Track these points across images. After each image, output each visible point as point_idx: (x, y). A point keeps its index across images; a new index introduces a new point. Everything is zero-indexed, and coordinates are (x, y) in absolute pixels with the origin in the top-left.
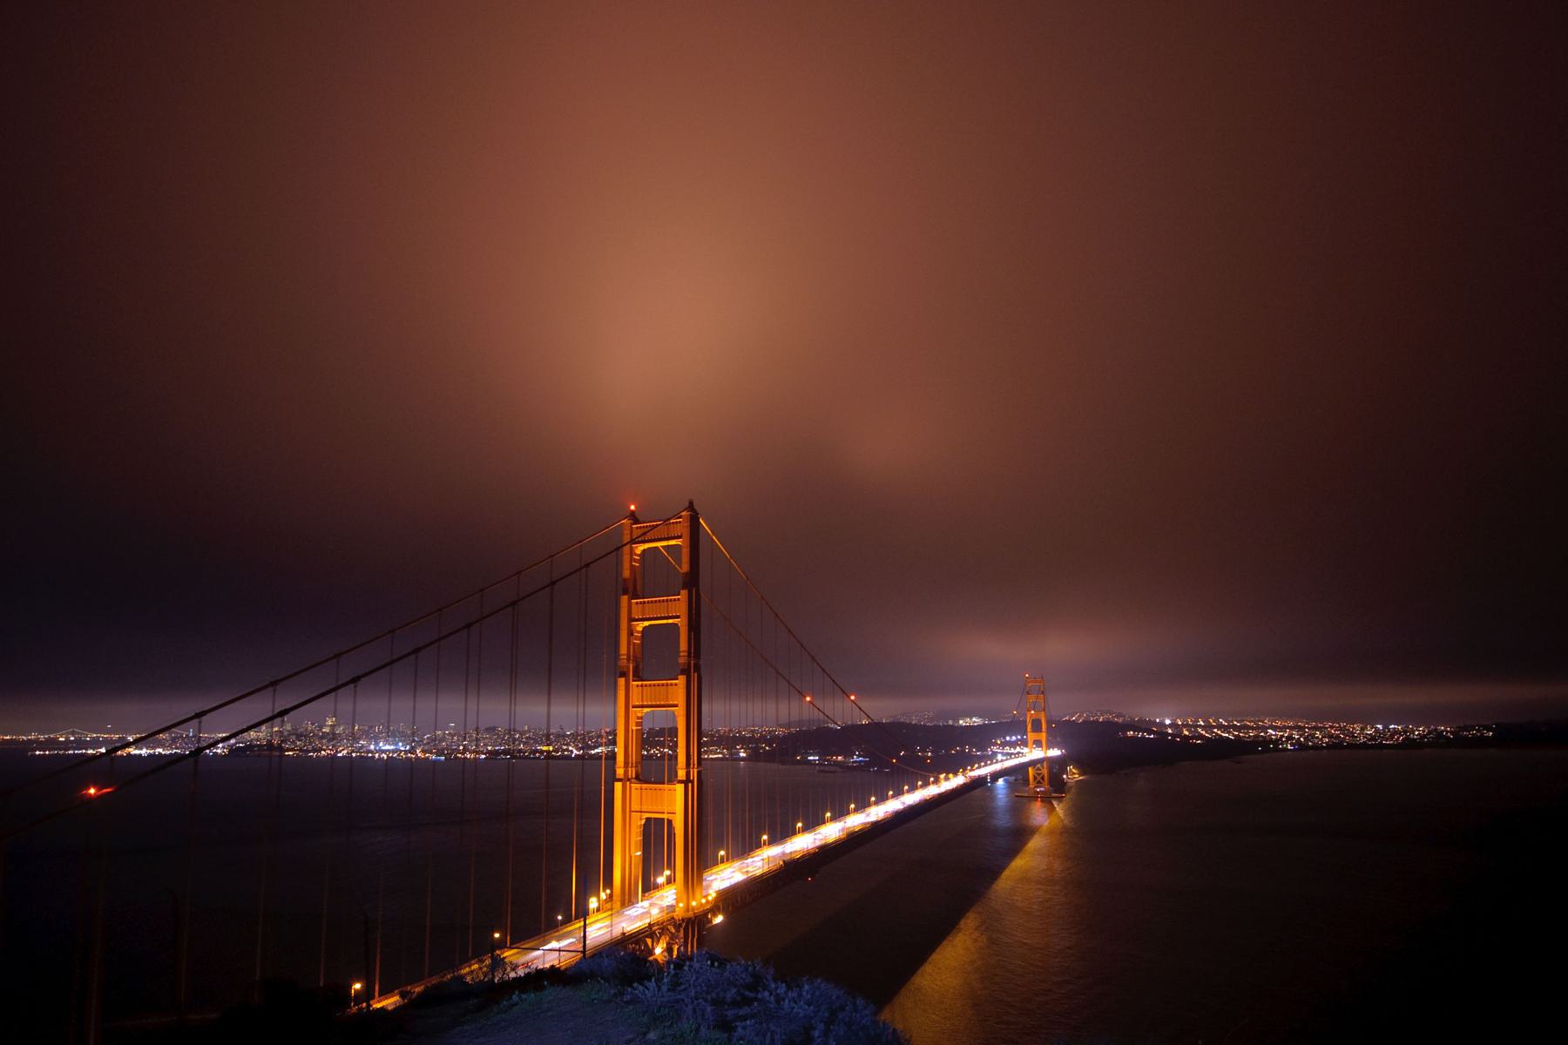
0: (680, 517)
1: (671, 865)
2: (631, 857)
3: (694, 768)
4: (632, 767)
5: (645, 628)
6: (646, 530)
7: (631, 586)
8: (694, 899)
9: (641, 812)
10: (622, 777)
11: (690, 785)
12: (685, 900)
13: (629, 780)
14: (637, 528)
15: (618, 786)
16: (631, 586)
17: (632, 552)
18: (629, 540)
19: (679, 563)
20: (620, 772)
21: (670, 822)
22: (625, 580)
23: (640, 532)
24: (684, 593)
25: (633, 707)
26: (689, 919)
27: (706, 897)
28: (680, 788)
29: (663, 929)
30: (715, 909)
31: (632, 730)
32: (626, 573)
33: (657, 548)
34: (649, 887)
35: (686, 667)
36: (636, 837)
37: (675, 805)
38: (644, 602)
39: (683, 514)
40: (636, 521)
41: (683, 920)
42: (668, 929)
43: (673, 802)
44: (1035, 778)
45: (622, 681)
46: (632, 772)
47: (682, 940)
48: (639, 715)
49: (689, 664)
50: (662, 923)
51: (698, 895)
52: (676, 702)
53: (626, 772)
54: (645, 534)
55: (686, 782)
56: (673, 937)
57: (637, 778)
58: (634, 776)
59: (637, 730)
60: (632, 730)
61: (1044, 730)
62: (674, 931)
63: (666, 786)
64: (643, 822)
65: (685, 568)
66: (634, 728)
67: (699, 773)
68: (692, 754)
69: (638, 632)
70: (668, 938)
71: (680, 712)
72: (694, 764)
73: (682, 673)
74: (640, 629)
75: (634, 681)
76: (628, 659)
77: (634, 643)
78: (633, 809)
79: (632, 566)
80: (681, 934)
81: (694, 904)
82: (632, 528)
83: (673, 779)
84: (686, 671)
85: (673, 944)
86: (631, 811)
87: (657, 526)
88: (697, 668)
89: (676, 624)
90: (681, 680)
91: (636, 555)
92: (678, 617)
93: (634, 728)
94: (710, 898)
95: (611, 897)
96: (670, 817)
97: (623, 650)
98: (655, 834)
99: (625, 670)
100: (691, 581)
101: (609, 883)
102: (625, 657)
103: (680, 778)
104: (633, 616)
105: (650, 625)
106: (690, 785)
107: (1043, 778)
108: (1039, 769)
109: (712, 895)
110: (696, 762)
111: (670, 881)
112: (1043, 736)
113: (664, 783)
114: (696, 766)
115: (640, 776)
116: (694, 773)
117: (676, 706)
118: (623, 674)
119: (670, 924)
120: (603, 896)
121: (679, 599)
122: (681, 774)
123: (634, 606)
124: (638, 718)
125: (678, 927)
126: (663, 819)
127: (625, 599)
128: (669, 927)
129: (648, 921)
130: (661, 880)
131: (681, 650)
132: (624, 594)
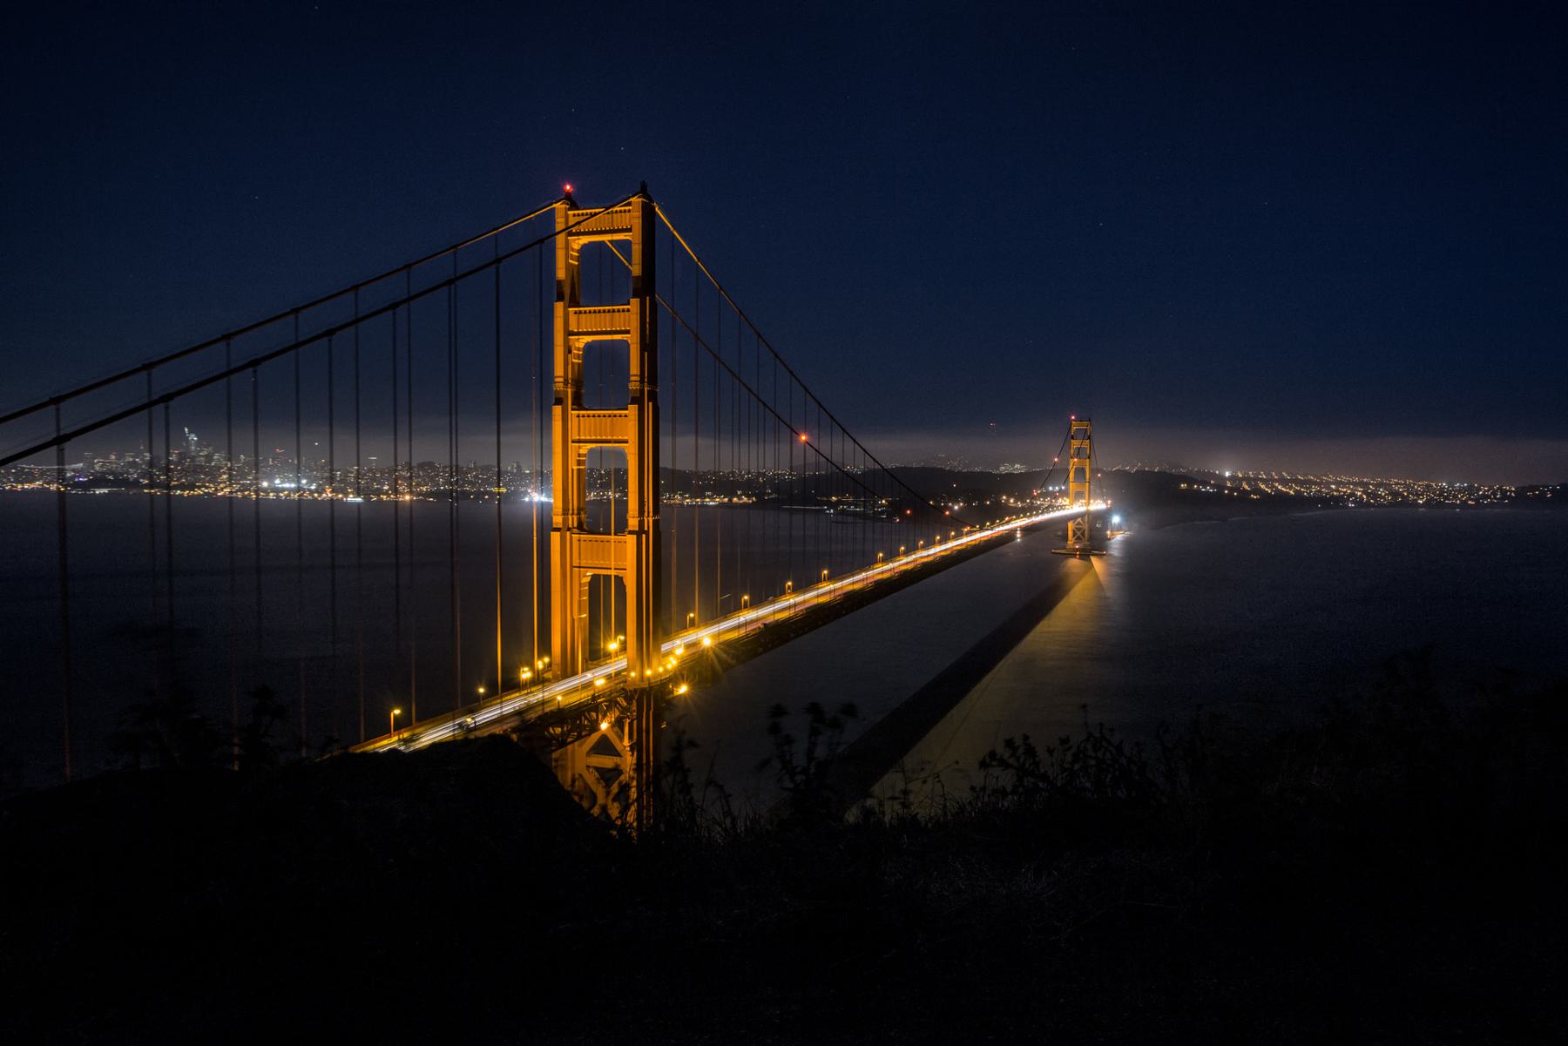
0: (629, 204)
1: (621, 627)
2: (573, 620)
3: (648, 516)
4: (573, 514)
5: (588, 346)
6: (581, 218)
7: (567, 291)
8: (650, 666)
9: (580, 567)
10: (560, 526)
11: (644, 536)
12: (638, 668)
13: (569, 529)
14: (574, 215)
15: (555, 537)
16: (567, 291)
17: (567, 246)
18: (564, 227)
19: (629, 259)
20: (558, 520)
21: (619, 580)
22: (559, 283)
23: (578, 219)
24: (635, 304)
25: (572, 442)
26: (643, 690)
27: (664, 666)
28: (631, 540)
29: (610, 701)
30: (676, 678)
31: (573, 470)
32: (561, 274)
33: (602, 243)
34: (595, 656)
35: (638, 395)
38: (580, 312)
39: (631, 200)
40: (574, 206)
41: (635, 691)
42: (618, 702)
43: (621, 555)
44: (1074, 534)
45: (557, 410)
46: (573, 521)
47: (635, 714)
48: (582, 451)
49: (642, 391)
50: (610, 695)
51: (655, 662)
52: (626, 438)
53: (565, 521)
54: (579, 223)
56: (624, 710)
57: (581, 528)
58: (575, 525)
59: (579, 470)
60: (573, 470)
62: (625, 704)
63: (613, 537)
64: (588, 579)
65: (636, 270)
66: (575, 467)
67: (656, 523)
68: (646, 500)
69: (579, 349)
70: (617, 713)
71: (631, 450)
72: (648, 512)
73: (634, 401)
74: (582, 346)
75: (572, 410)
76: (566, 382)
77: (573, 363)
78: (574, 565)
79: (567, 262)
80: (634, 708)
81: (648, 673)
82: (567, 216)
83: (622, 528)
84: (637, 400)
85: (624, 718)
86: (572, 567)
87: (596, 214)
88: (653, 396)
89: (627, 341)
90: (633, 410)
91: (573, 250)
92: (628, 332)
93: (575, 467)
94: (669, 667)
95: (550, 665)
96: (620, 574)
97: (559, 370)
98: (600, 591)
99: (562, 396)
100: (645, 287)
101: (545, 648)
102: (562, 380)
103: (630, 528)
104: (570, 329)
105: (593, 341)
106: (644, 536)
107: (1083, 534)
108: (1079, 523)
109: (672, 663)
110: (651, 510)
111: (624, 648)
113: (610, 534)
114: (651, 514)
115: (585, 527)
116: (649, 521)
117: (626, 442)
118: (559, 401)
119: (618, 696)
120: (540, 665)
121: (628, 310)
122: (633, 523)
123: (573, 319)
124: (579, 455)
125: (629, 699)
126: (610, 576)
127: (559, 307)
128: (618, 699)
129: (592, 692)
130: (613, 646)
131: (631, 373)
132: (557, 301)
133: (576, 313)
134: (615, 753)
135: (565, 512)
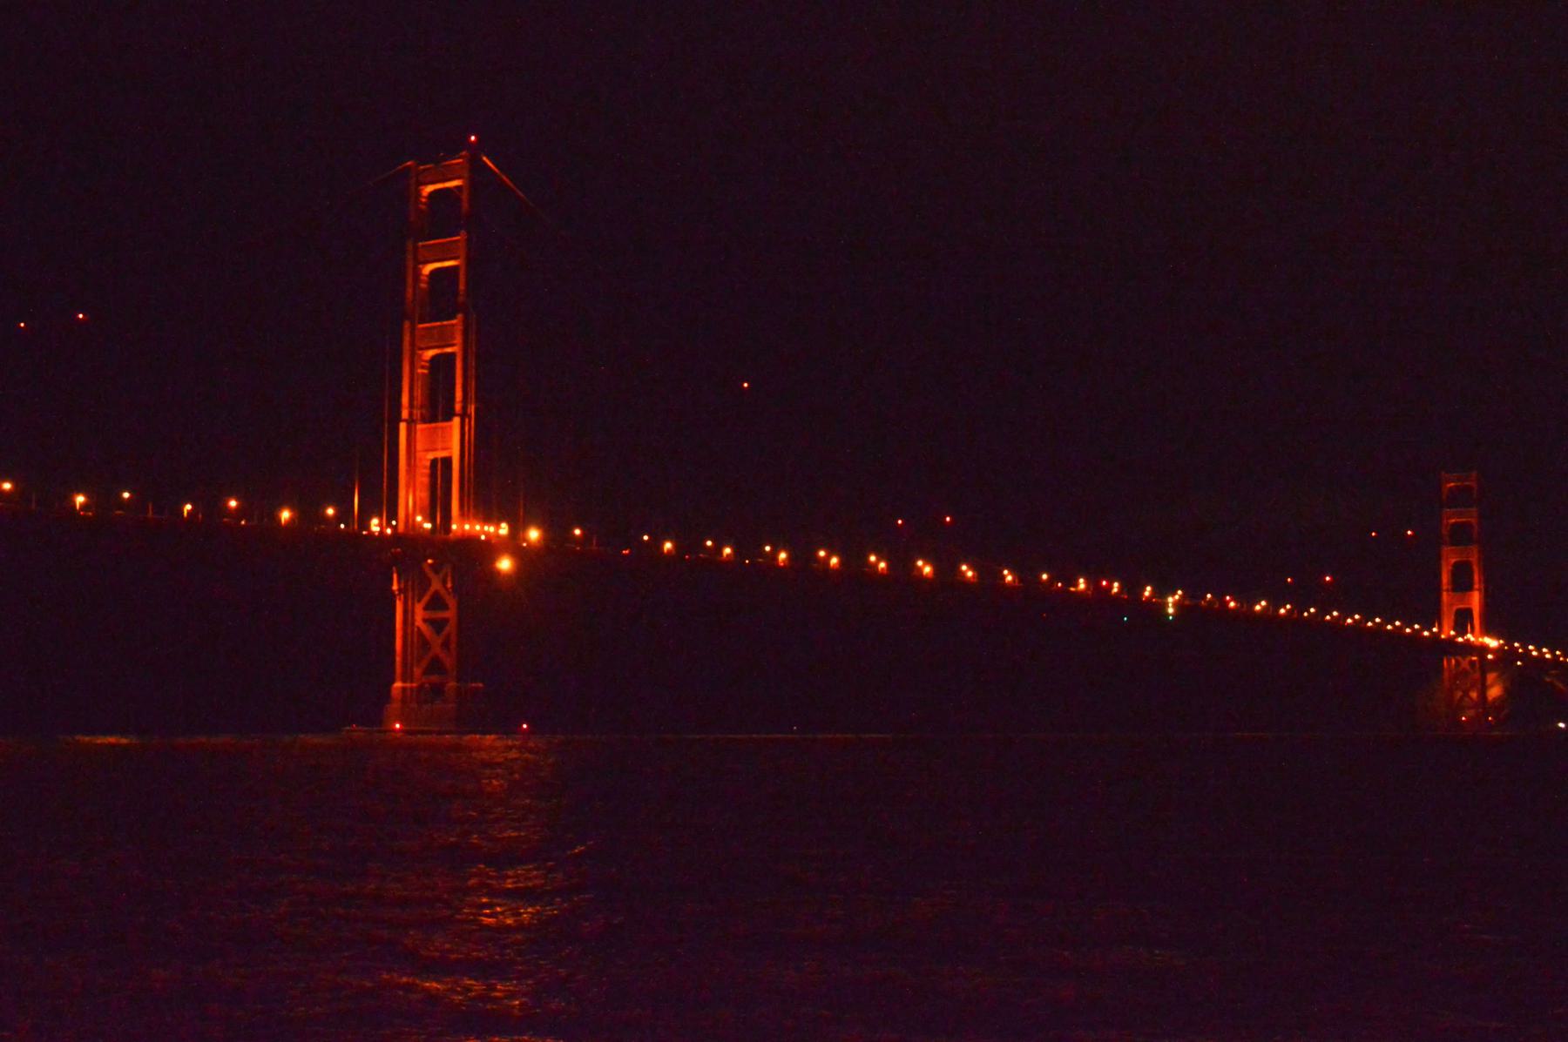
11: (467, 420)
15: (403, 426)
20: (405, 414)
21: (447, 462)
24: (463, 232)
28: (457, 420)
36: (423, 478)
37: (451, 440)
39: (464, 153)
43: (447, 434)
46: (417, 412)
53: (411, 414)
55: (464, 415)
61: (1476, 586)
64: (428, 464)
112: (1475, 600)
116: (472, 409)
122: (458, 407)
133: (423, 246)
134: (445, 607)
135: (411, 406)
